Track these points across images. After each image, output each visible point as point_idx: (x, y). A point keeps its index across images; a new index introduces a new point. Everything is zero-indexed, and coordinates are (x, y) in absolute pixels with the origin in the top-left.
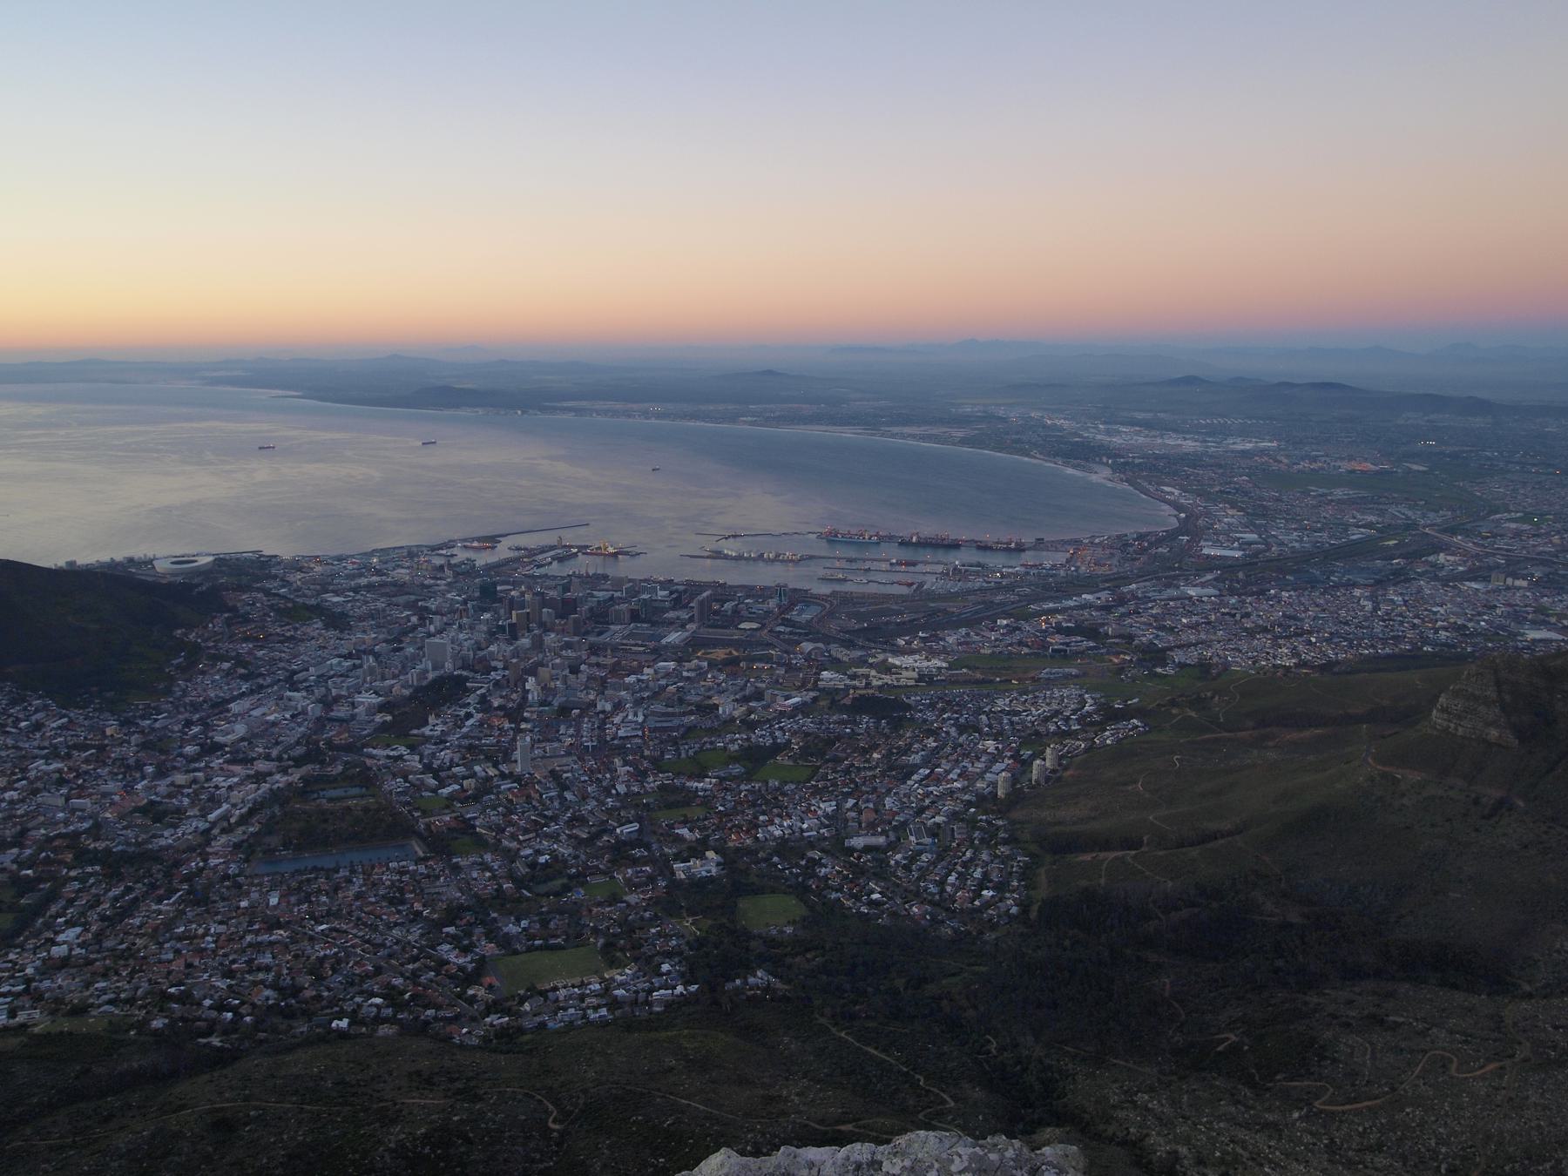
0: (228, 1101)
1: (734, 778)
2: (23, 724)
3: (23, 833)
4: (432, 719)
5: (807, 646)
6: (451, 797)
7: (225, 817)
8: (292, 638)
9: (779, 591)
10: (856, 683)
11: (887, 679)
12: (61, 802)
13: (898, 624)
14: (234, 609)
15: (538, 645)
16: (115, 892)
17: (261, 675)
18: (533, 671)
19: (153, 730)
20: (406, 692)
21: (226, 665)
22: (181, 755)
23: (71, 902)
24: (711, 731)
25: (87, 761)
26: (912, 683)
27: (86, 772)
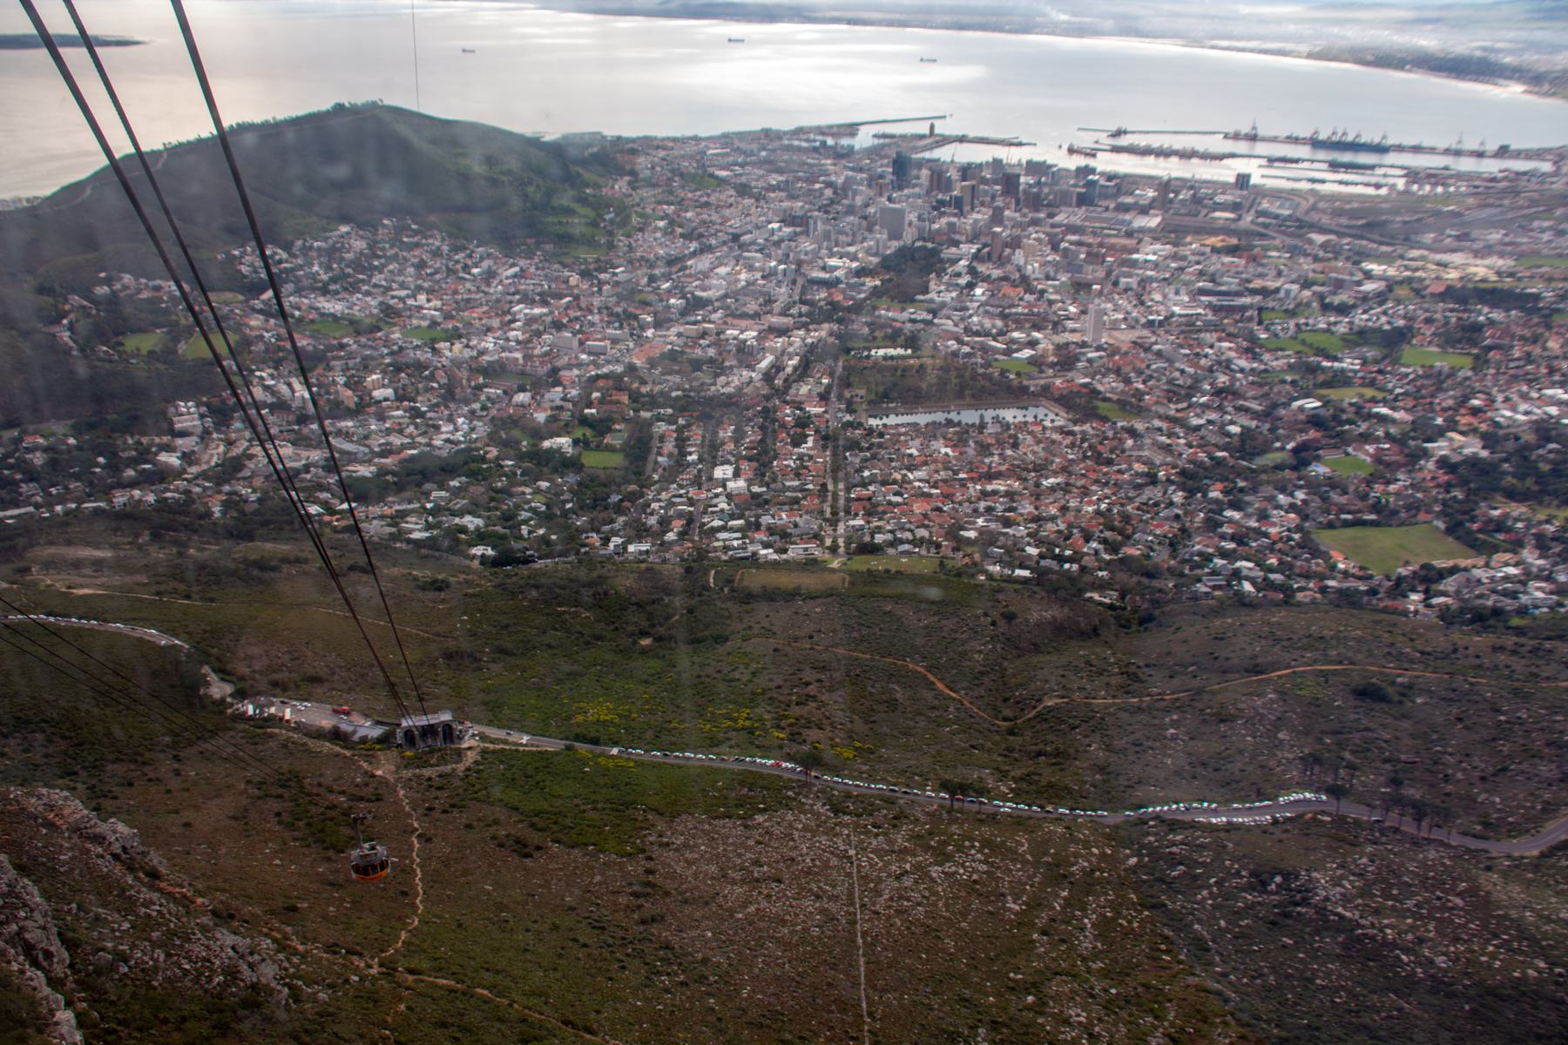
0: (1315, 662)
1: (1376, 362)
2: (475, 271)
3: (555, 371)
4: (932, 285)
5: (1319, 238)
6: (1032, 361)
7: (777, 367)
8: (707, 205)
9: (1243, 180)
10: (1418, 274)
11: (1453, 275)
12: (575, 344)
13: (1405, 223)
14: (633, 173)
15: (997, 218)
16: (727, 433)
17: (701, 236)
18: (1015, 243)
19: (617, 283)
20: (875, 260)
21: (661, 224)
22: (668, 307)
23: (681, 443)
24: (1292, 314)
25: (568, 307)
26: (1494, 278)
27: (577, 319)
